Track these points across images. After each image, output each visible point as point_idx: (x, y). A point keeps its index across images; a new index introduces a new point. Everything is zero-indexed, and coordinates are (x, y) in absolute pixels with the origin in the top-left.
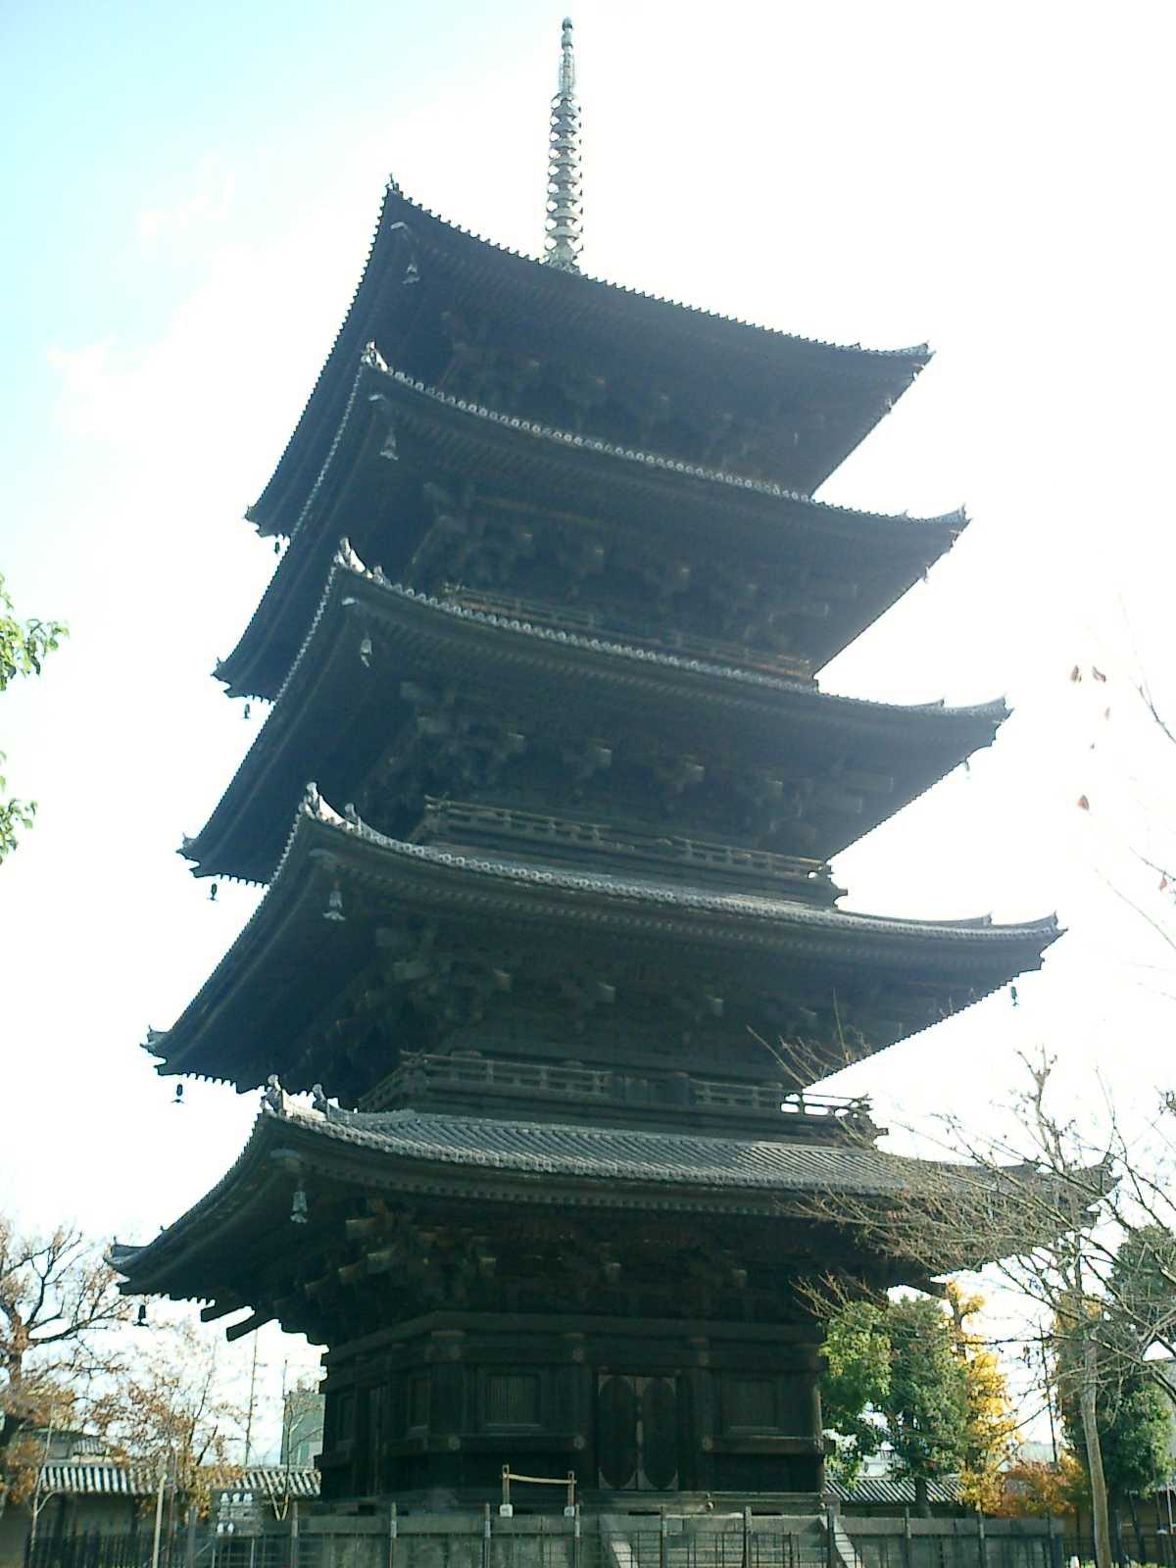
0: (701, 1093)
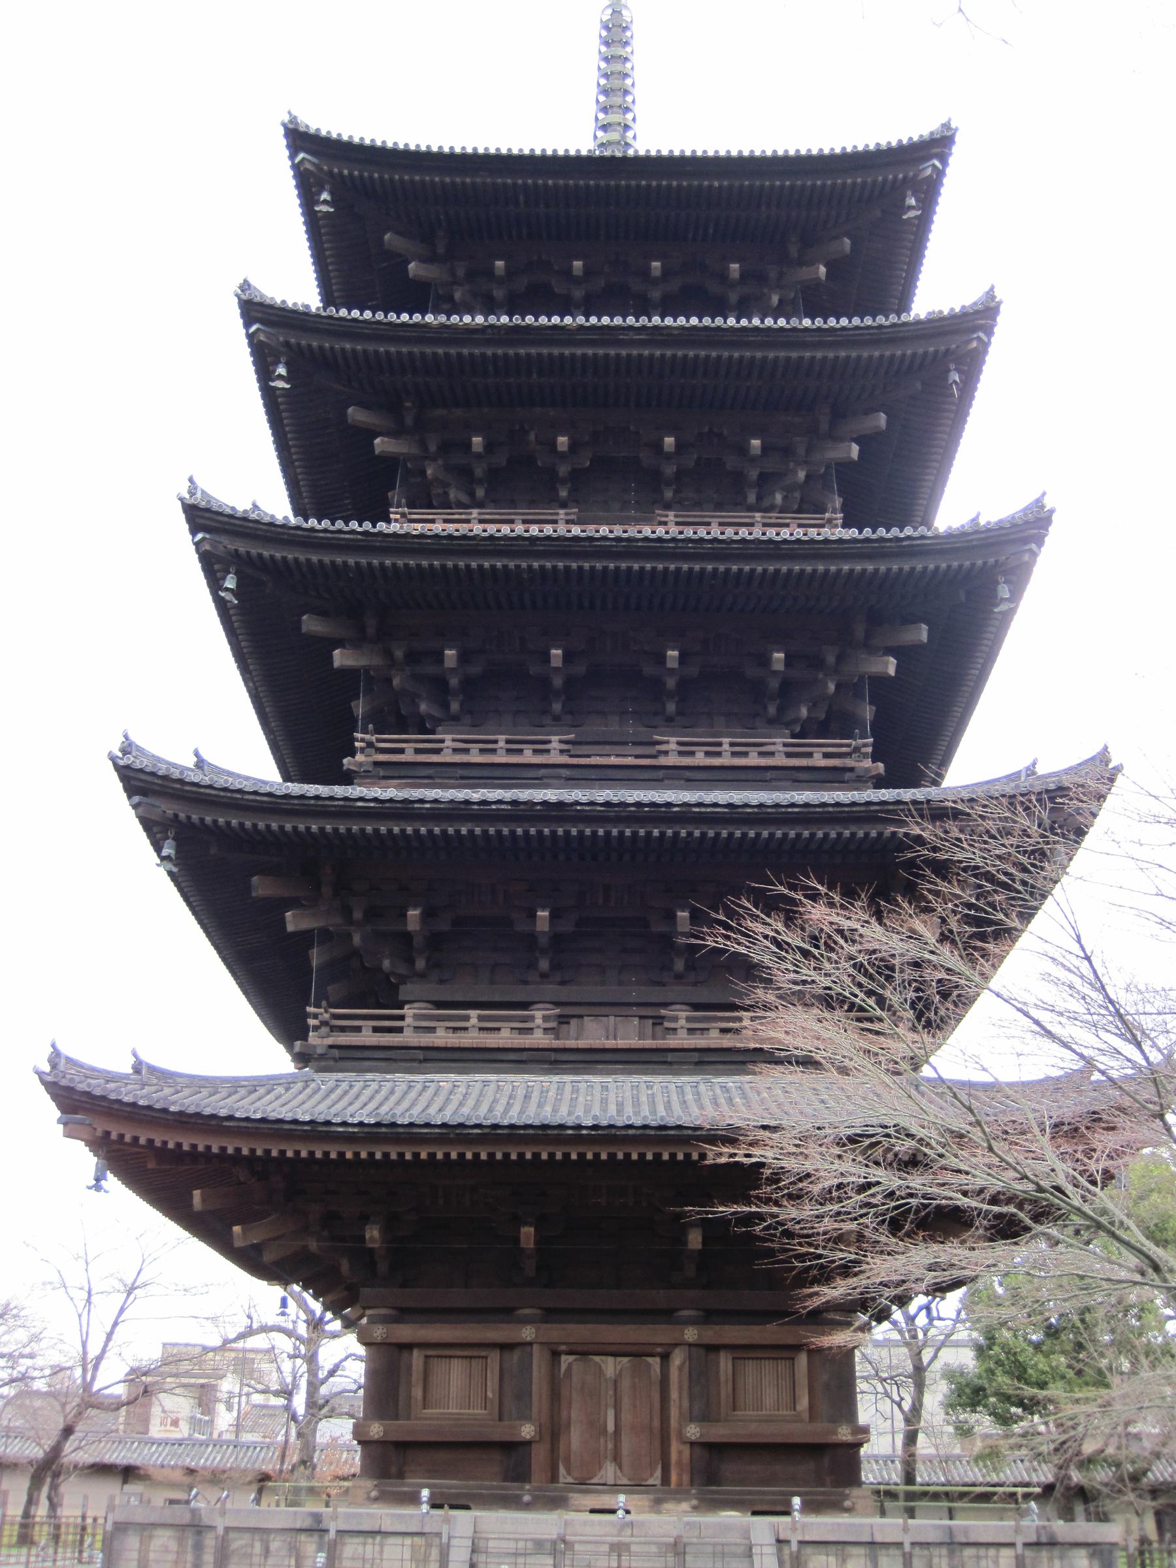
0: (672, 1025)
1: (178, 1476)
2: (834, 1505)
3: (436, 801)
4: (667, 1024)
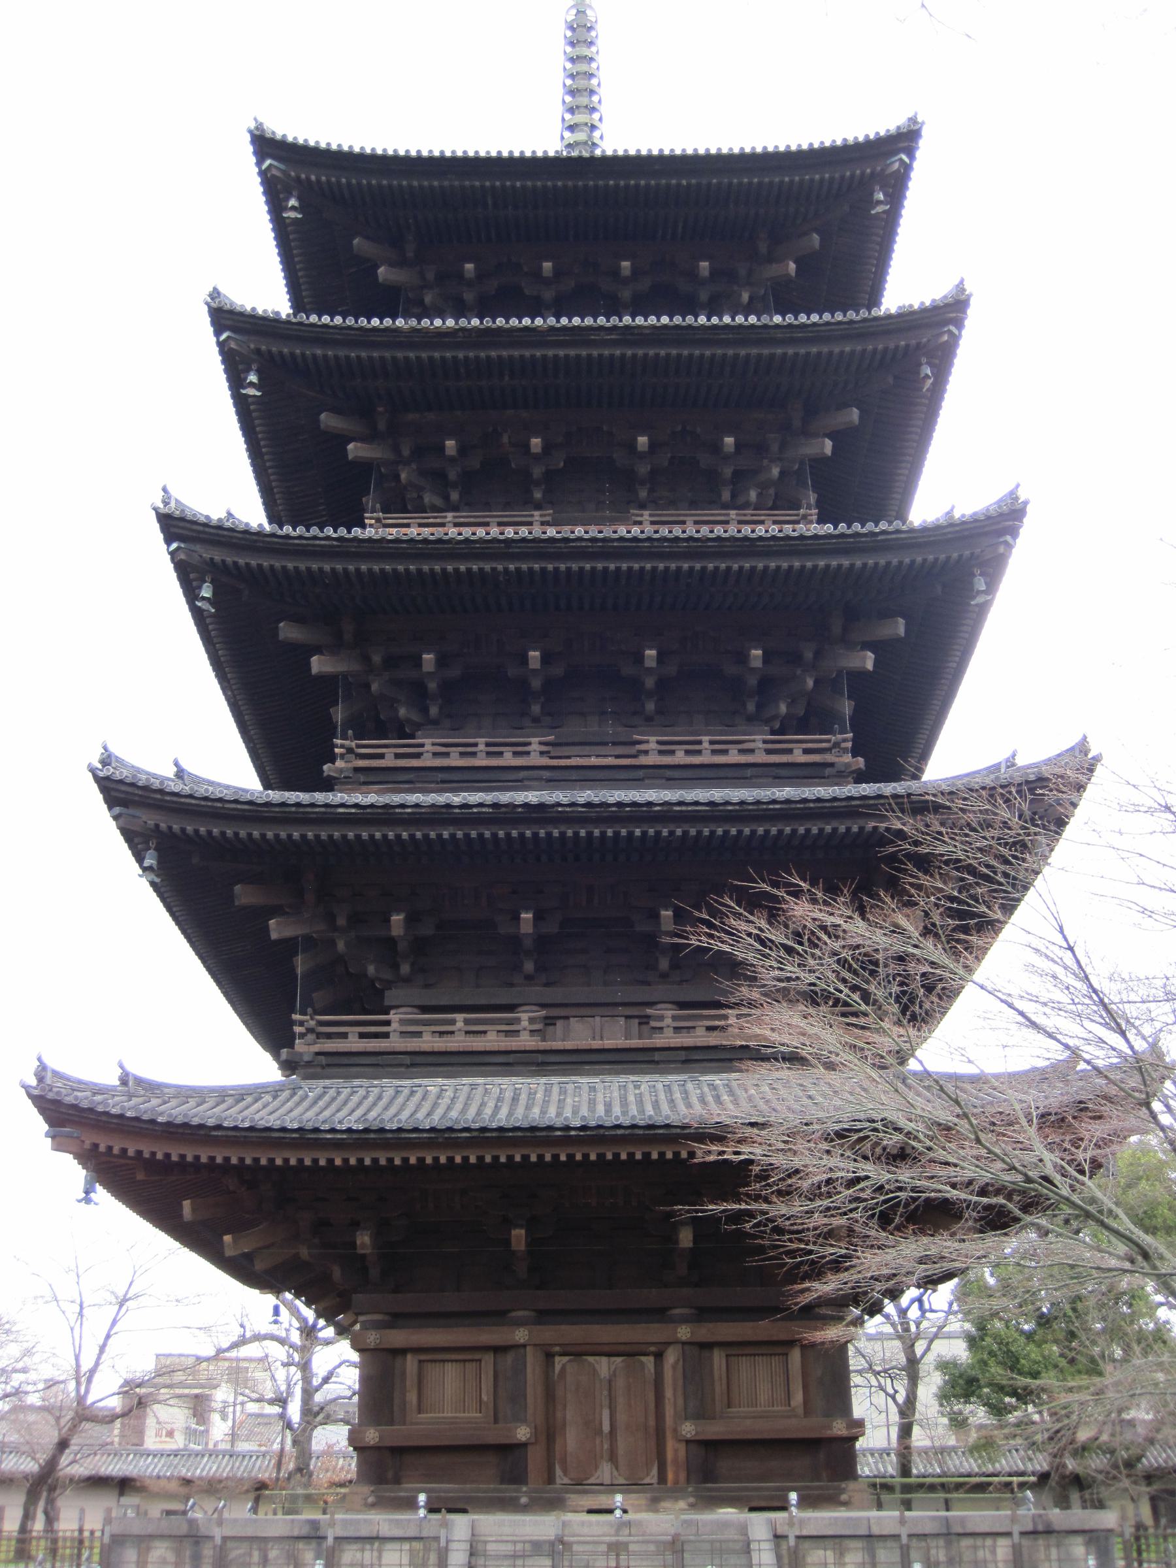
1: (174, 1486)
2: (831, 1500)
3: (417, 806)
4: (653, 1024)
